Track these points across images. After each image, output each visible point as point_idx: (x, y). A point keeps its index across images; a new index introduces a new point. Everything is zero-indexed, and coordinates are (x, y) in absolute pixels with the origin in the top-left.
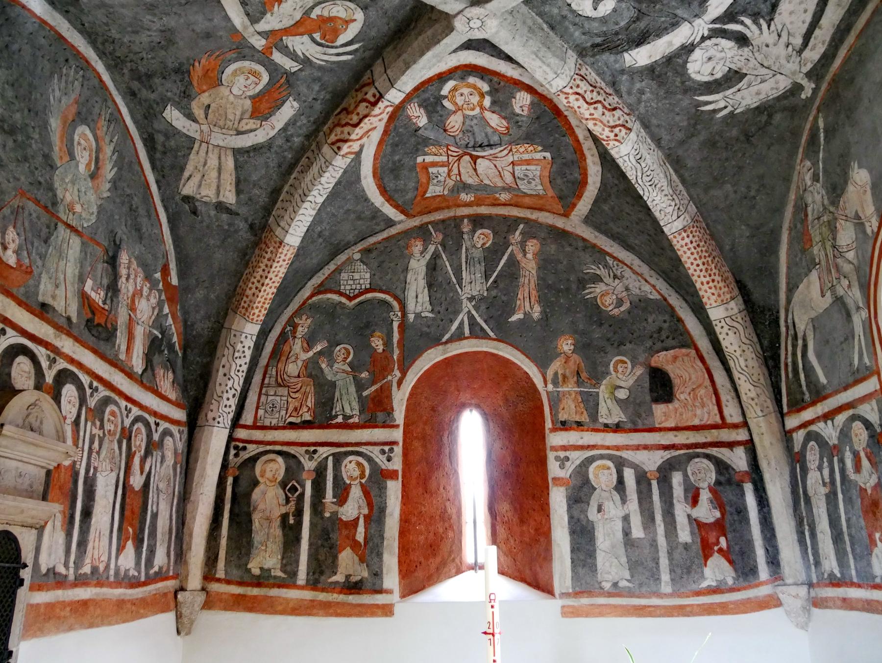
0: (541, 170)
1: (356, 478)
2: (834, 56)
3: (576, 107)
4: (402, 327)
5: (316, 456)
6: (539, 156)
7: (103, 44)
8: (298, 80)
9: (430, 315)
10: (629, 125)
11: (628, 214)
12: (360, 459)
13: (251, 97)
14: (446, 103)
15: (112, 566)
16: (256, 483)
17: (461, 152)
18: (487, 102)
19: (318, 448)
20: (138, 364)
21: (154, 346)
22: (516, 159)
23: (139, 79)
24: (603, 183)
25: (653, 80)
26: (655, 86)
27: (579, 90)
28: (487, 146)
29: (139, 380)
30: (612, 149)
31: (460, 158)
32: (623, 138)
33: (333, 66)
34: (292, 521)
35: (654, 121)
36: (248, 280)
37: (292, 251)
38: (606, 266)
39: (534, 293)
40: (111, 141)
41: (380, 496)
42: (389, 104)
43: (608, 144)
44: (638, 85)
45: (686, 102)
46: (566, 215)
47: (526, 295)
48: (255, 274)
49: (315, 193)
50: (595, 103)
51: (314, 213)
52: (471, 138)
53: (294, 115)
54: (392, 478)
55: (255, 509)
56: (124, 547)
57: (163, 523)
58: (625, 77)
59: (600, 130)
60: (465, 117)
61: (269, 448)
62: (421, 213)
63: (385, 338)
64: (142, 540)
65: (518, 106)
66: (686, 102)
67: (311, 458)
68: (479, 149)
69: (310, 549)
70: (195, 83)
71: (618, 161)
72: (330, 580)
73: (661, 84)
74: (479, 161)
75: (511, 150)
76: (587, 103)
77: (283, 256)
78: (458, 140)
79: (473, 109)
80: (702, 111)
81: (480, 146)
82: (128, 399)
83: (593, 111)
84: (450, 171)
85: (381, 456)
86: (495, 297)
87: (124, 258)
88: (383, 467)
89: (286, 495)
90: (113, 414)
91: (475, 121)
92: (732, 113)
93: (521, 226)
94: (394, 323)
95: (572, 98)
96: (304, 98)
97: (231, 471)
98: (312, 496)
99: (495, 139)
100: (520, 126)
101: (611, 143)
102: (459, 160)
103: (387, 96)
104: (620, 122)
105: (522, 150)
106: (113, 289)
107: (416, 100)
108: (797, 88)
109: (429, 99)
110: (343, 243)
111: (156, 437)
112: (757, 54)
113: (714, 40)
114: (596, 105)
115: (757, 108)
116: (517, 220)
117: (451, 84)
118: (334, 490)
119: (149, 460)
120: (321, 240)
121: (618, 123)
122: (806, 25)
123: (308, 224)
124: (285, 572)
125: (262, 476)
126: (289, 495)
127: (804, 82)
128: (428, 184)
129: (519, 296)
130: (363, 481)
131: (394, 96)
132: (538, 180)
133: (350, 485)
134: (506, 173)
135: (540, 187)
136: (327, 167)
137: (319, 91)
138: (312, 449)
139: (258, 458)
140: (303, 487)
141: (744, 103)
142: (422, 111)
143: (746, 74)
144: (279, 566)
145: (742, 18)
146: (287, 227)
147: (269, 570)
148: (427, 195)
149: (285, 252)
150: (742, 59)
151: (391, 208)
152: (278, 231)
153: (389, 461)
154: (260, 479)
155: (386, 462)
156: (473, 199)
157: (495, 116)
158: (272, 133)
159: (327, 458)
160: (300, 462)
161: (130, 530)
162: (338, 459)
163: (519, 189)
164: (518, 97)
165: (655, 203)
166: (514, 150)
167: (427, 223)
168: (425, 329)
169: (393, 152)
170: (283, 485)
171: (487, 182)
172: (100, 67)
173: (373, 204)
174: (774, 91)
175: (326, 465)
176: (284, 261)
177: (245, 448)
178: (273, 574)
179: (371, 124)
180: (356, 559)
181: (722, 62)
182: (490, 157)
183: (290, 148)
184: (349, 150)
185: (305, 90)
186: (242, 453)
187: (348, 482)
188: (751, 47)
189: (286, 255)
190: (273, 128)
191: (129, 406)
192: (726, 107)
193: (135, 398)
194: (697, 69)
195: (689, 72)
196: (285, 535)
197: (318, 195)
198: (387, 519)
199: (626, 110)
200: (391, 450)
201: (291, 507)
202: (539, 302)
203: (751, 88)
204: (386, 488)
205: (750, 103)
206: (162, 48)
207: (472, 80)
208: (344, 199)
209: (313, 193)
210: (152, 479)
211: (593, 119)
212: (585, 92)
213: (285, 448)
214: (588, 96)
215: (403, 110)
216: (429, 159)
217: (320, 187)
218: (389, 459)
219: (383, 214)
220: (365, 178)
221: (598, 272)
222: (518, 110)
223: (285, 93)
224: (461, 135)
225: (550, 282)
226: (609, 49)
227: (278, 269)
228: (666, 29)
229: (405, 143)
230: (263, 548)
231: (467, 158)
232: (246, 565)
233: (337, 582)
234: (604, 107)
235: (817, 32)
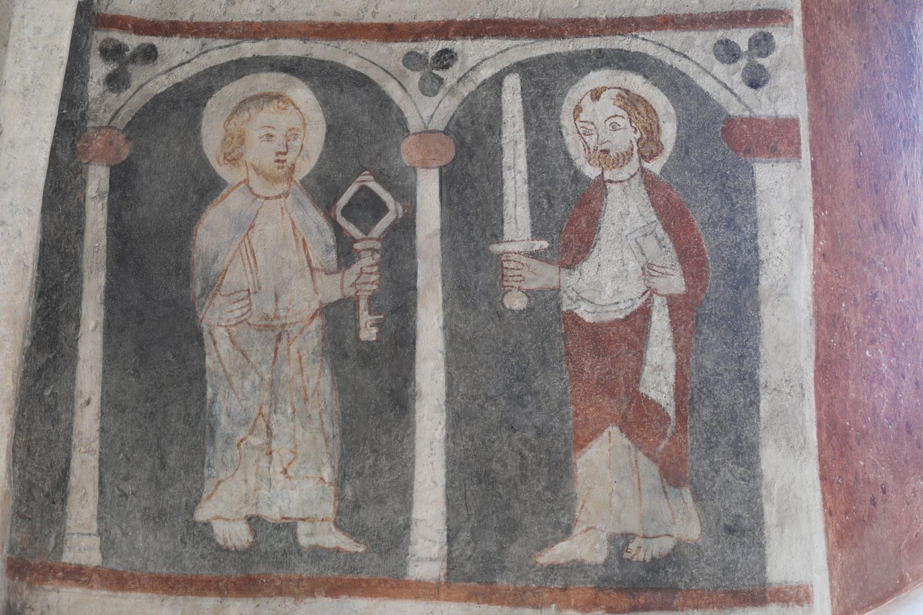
1: (626, 157)
5: (450, 76)
12: (636, 83)
19: (457, 45)
34: (369, 333)
41: (730, 223)
54: (773, 152)
55: (212, 288)
61: (249, 49)
67: (431, 86)
69: (452, 436)
72: (546, 558)
85: (719, 69)
88: (735, 110)
89: (338, 230)
97: (98, 143)
98: (446, 231)
118: (534, 205)
124: (355, 532)
125: (233, 160)
126: (352, 230)
130: (655, 167)
133: (601, 184)
138: (432, 47)
139: (210, 91)
140: (407, 196)
144: (329, 509)
147: (288, 526)
153: (755, 84)
154: (223, 171)
155: (742, 89)
159: (497, 81)
160: (385, 101)
175: (497, 113)
177: (149, 54)
178: (304, 541)
180: (650, 471)
186: (139, 74)
187: (591, 172)
196: (342, 386)
198: (766, 311)
200: (763, 44)
204: (751, 191)
213: (320, 50)
218: (756, 80)
230: (255, 441)
232: (191, 509)
233: (578, 566)
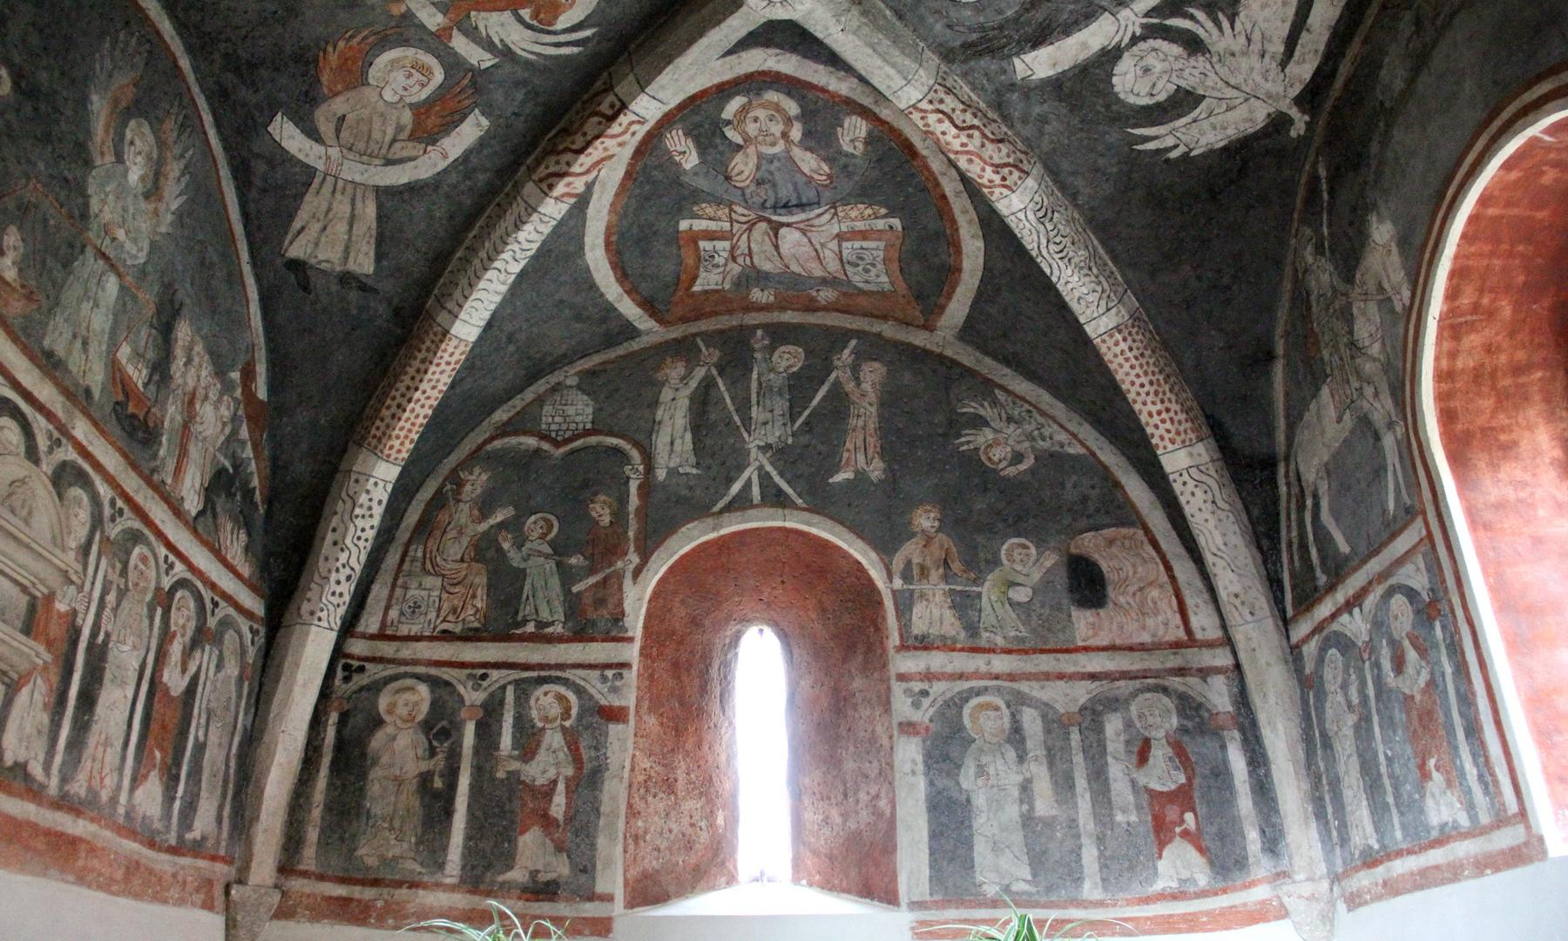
2: (1333, 74)
3: (938, 133)
4: (646, 489)
7: (186, 10)
9: (694, 471)
10: (1026, 167)
15: (123, 799)
16: (378, 722)
20: (193, 504)
21: (221, 483)
23: (237, 70)
25: (1061, 100)
27: (942, 107)
29: (192, 526)
32: (1016, 184)
35: (1065, 165)
36: (386, 394)
37: (462, 348)
38: (995, 403)
39: (871, 441)
40: (182, 156)
43: (992, 193)
45: (1113, 136)
47: (860, 443)
48: (399, 385)
49: (506, 256)
50: (972, 127)
51: (504, 289)
56: (145, 777)
57: (214, 757)
59: (978, 170)
63: (615, 505)
64: (176, 778)
66: (1113, 136)
70: (325, 79)
71: (1008, 220)
76: (956, 126)
77: (446, 357)
80: (1140, 151)
82: (170, 546)
83: (965, 140)
86: (807, 446)
87: (183, 332)
90: (144, 559)
92: (1185, 156)
94: (631, 482)
95: (932, 118)
101: (997, 191)
103: (633, 106)
104: (1011, 160)
106: (161, 370)
108: (1279, 123)
111: (212, 622)
112: (1217, 67)
113: (1151, 43)
114: (971, 132)
115: (1225, 149)
119: (198, 654)
121: (1006, 160)
122: (1288, 25)
123: (493, 307)
127: (1294, 112)
129: (848, 445)
131: (647, 108)
136: (530, 215)
141: (1203, 141)
143: (1204, 97)
145: (1191, 10)
146: (456, 309)
149: (450, 350)
150: (1196, 73)
152: (442, 317)
161: (158, 754)
162: (524, 690)
168: (684, 492)
170: (427, 726)
172: (176, 45)
174: (1248, 125)
176: (448, 363)
181: (1166, 77)
188: (1208, 55)
189: (452, 354)
191: (172, 558)
192: (1176, 146)
193: (182, 548)
194: (1128, 86)
195: (1116, 89)
197: (510, 259)
199: (1020, 145)
201: (439, 762)
202: (882, 457)
203: (1212, 119)
205: (1213, 140)
206: (278, 21)
209: (503, 256)
210: (200, 689)
211: (967, 152)
212: (953, 110)
214: (958, 117)
217: (516, 247)
221: (982, 412)
225: (900, 425)
227: (437, 376)
228: (1076, 22)
234: (984, 136)
235: (1304, 37)
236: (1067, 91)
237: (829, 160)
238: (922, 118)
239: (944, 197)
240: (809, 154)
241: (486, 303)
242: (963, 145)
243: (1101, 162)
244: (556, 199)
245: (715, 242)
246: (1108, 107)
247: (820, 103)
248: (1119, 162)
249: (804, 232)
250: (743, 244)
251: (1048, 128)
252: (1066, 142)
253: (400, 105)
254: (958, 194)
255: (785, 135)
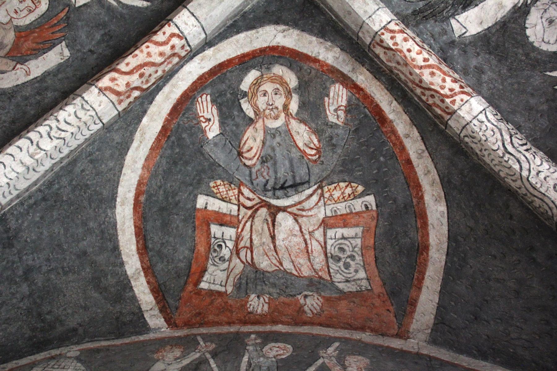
0: (363, 237)
6: (358, 205)
8: (79, 20)
11: (498, 280)
13: (18, 29)
14: (246, 106)
17: (257, 201)
18: (294, 107)
22: (329, 214)
24: (452, 237)
25: (490, 53)
26: (494, 62)
28: (291, 186)
30: (459, 109)
31: (255, 210)
33: (124, 11)
42: (177, 31)
43: (453, 102)
44: (474, 62)
46: (402, 335)
52: (271, 173)
53: (60, 65)
58: (456, 52)
59: (440, 81)
60: (266, 130)
62: (188, 324)
65: (332, 108)
68: (279, 193)
73: (502, 58)
74: (280, 216)
75: (322, 195)
78: (254, 176)
79: (276, 118)
81: (283, 188)
84: (238, 238)
91: (278, 139)
93: (337, 344)
96: (79, 47)
99: (302, 172)
100: (334, 146)
102: (252, 217)
105: (337, 194)
107: (209, 91)
109: (225, 90)
110: (60, 329)
116: (329, 341)
117: (252, 75)
120: (25, 288)
128: (207, 259)
132: (358, 258)
134: (315, 243)
135: (362, 274)
137: (99, 43)
142: (215, 111)
148: (203, 285)
151: (147, 290)
156: (266, 307)
157: (302, 128)
158: (23, 79)
163: (333, 282)
164: (331, 95)
165: (542, 176)
166: (327, 195)
167: (195, 335)
169: (168, 173)
171: (287, 265)
173: (122, 264)
179: (149, 54)
182: (294, 210)
183: (39, 102)
184: (110, 84)
185: (84, 37)
190: (28, 74)
197: (45, 135)
207: (278, 70)
208: (84, 224)
211: (430, 66)
215: (192, 104)
216: (215, 205)
217: (53, 124)
219: (134, 298)
220: (123, 204)
222: (332, 119)
223: (58, 35)
224: (258, 167)
226: (433, 15)
229: (187, 163)
231: (263, 212)
236: (493, 44)
237: (317, 132)
238: (392, 38)
239: (409, 162)
240: (303, 127)
241: (8, 169)
242: (425, 60)
243: (532, 101)
244: (100, 90)
245: (224, 228)
246: (527, 55)
247: (313, 72)
248: (547, 101)
249: (296, 217)
250: (246, 234)
251: (485, 78)
252: (501, 87)
253: (7, 27)
254: (420, 156)
255: (286, 107)
